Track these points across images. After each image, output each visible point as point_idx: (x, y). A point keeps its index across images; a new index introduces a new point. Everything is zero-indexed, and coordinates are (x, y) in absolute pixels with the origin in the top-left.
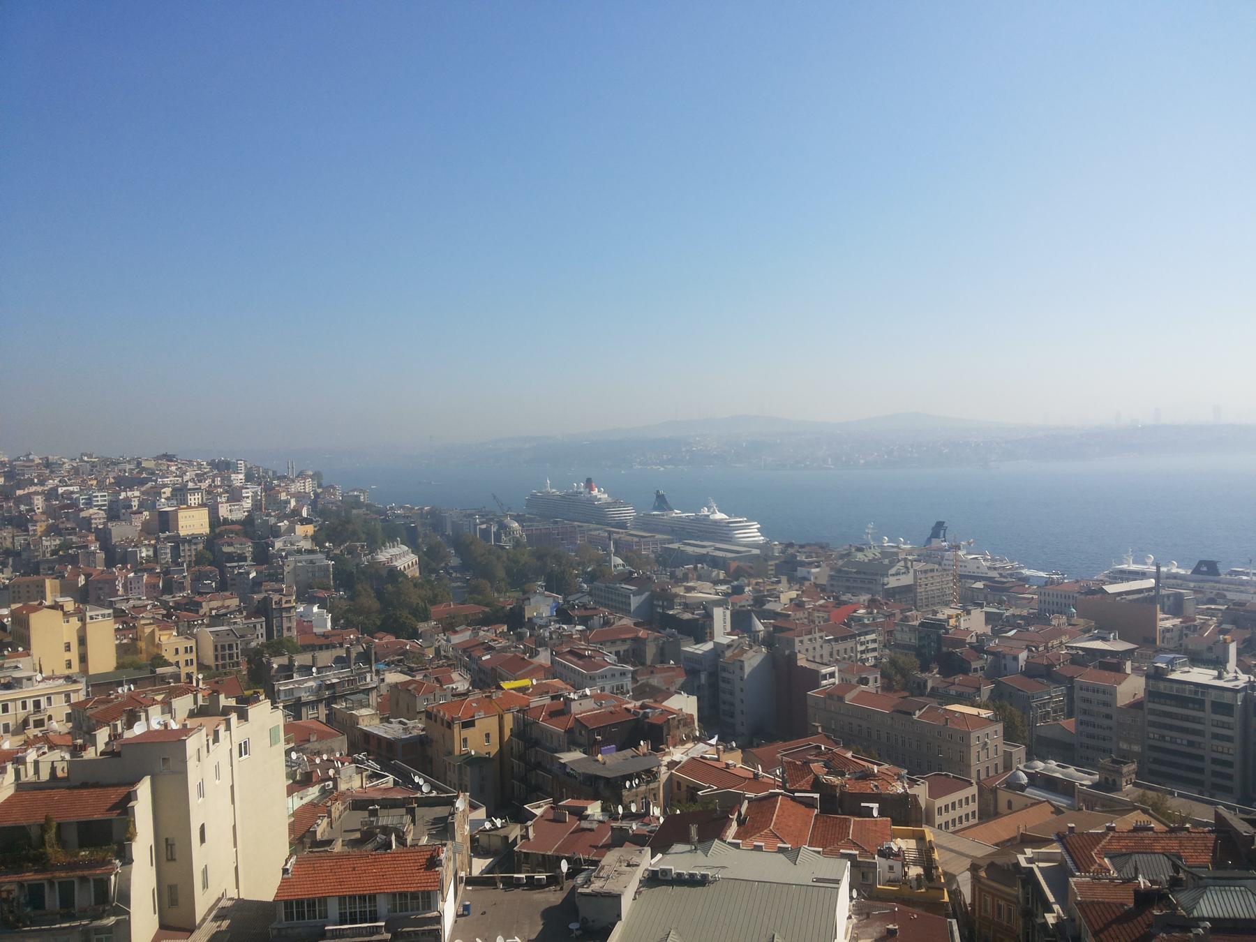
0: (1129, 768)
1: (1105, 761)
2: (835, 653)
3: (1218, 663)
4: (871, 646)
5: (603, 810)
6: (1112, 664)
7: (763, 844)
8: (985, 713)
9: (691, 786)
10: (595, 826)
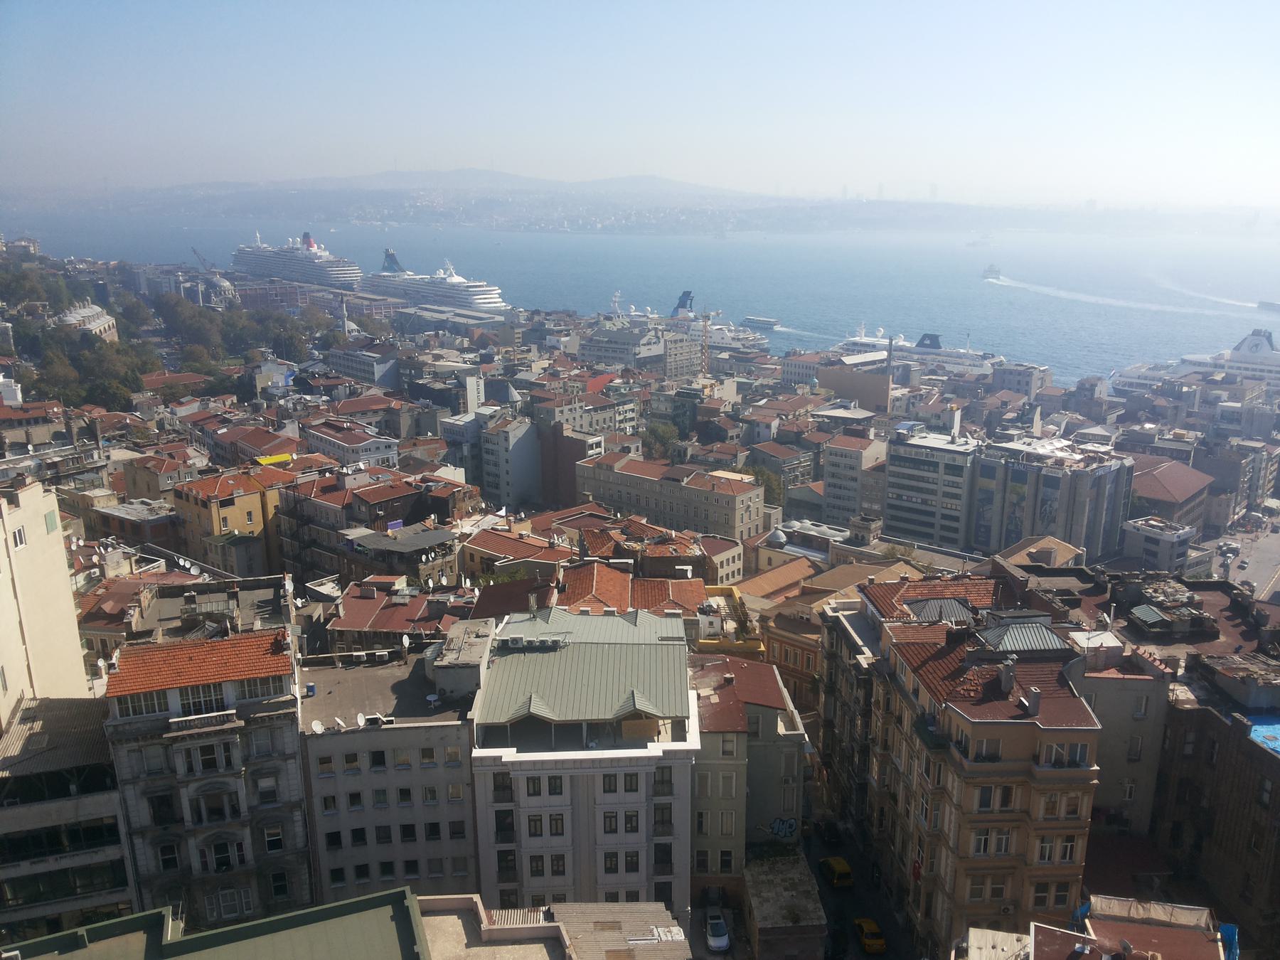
0: (877, 525)
1: (855, 519)
2: (594, 422)
3: (945, 429)
4: (630, 415)
5: (408, 585)
6: (856, 430)
7: (589, 609)
8: (748, 478)
9: (486, 557)
10: (407, 600)
